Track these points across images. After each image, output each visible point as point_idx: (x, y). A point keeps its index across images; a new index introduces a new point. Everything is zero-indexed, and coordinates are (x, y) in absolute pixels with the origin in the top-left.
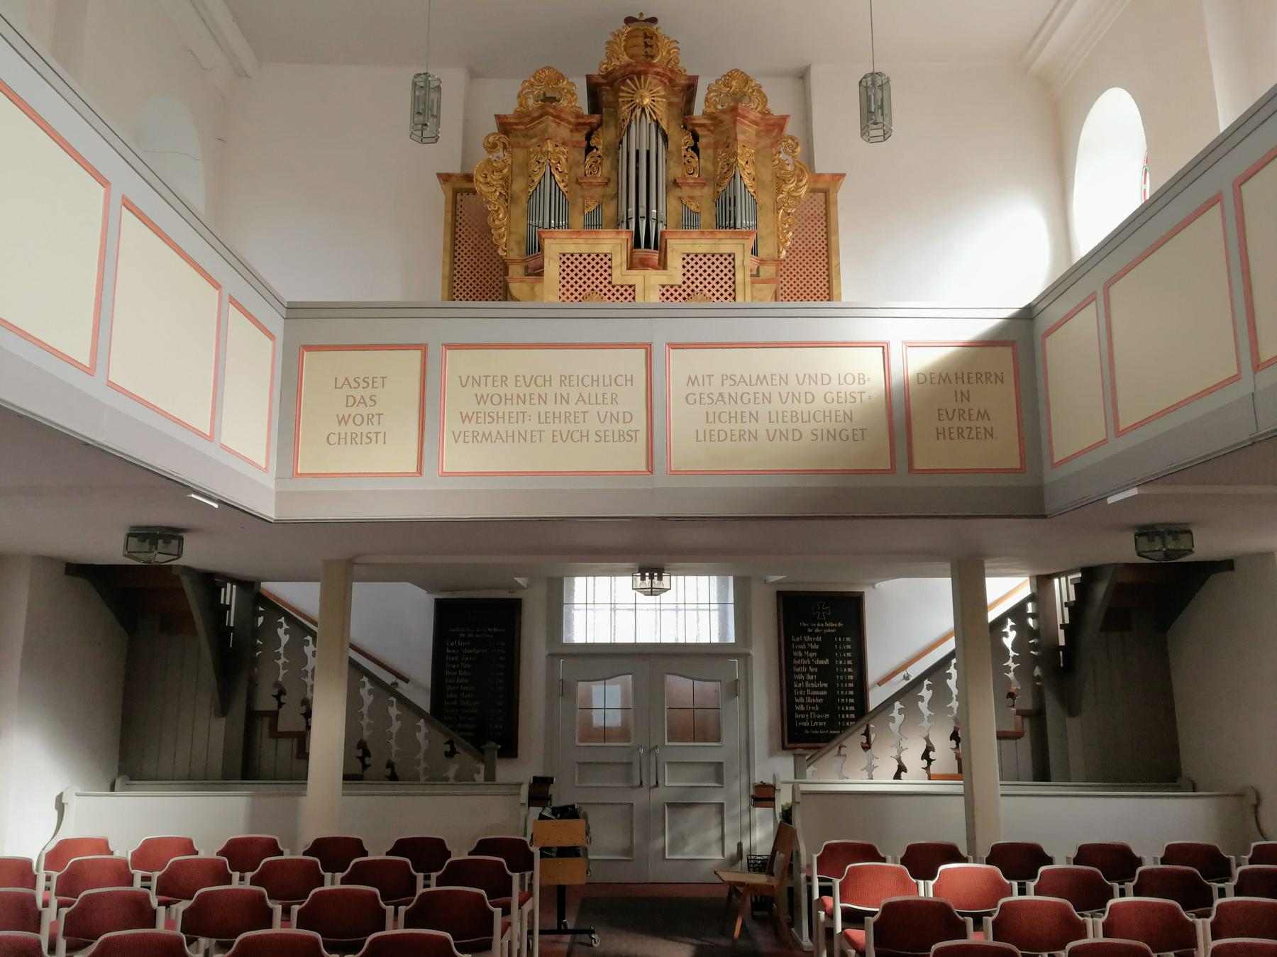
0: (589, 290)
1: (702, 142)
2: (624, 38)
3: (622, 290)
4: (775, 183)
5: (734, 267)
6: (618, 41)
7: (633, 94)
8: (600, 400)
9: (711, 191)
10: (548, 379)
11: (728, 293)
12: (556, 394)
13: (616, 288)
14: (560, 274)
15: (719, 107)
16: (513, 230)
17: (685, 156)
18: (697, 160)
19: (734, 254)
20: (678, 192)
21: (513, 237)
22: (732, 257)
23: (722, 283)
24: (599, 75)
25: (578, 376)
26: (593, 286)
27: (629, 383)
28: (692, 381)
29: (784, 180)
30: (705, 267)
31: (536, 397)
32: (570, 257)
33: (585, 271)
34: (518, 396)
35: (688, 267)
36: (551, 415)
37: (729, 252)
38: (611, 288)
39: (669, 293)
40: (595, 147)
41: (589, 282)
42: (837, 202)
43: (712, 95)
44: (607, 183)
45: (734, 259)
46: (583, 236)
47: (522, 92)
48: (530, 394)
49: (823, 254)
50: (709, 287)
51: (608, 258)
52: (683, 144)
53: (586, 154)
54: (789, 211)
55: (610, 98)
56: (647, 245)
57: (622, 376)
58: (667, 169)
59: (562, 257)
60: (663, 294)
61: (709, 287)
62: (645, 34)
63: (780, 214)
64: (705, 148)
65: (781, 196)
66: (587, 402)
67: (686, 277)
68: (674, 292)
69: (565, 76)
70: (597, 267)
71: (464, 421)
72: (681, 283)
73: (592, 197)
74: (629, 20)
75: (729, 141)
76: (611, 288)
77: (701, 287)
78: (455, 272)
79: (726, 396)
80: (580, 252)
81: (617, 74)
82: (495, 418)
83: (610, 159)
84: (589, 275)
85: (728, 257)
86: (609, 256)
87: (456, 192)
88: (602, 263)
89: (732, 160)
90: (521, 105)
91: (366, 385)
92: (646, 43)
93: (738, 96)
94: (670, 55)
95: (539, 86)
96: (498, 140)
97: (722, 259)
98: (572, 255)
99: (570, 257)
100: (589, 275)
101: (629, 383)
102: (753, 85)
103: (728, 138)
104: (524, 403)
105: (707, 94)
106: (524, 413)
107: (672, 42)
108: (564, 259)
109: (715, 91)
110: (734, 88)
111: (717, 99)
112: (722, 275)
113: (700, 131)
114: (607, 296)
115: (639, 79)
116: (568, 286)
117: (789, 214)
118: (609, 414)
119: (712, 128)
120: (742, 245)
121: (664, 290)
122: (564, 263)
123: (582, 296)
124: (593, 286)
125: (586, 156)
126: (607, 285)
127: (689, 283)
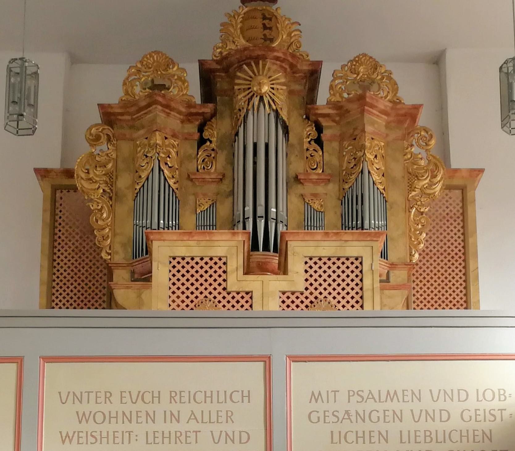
0: (201, 297)
1: (327, 134)
2: (240, 20)
3: (238, 297)
4: (406, 179)
5: (361, 272)
6: (234, 23)
7: (251, 81)
8: (214, 418)
10: (156, 394)
11: (355, 300)
12: (165, 412)
13: (231, 295)
14: (170, 279)
16: (118, 231)
17: (307, 150)
18: (321, 153)
19: (362, 257)
20: (299, 189)
21: (118, 239)
22: (360, 260)
23: (348, 289)
24: (213, 60)
25: (189, 392)
26: (206, 293)
27: (246, 399)
28: (315, 397)
29: (417, 176)
30: (330, 272)
31: (143, 415)
32: (181, 261)
33: (197, 276)
34: (124, 413)
35: (311, 272)
36: (159, 435)
38: (226, 295)
39: (290, 300)
40: (208, 139)
41: (202, 289)
42: (475, 200)
43: (337, 82)
44: (221, 179)
45: (361, 263)
46: (195, 238)
47: (127, 78)
48: (137, 412)
49: (460, 257)
50: (334, 294)
52: (306, 136)
54: (422, 210)
55: (225, 86)
56: (266, 248)
57: (238, 391)
58: (288, 164)
59: (172, 260)
60: (283, 302)
61: (334, 294)
63: (413, 213)
64: (330, 140)
65: (413, 193)
66: (200, 421)
67: (309, 282)
68: (295, 300)
69: (175, 60)
70: (211, 272)
71: (63, 442)
72: (303, 289)
73: (205, 195)
75: (356, 133)
76: (226, 295)
77: (325, 293)
78: (54, 277)
79: (353, 413)
80: (192, 255)
81: (233, 59)
82: (98, 438)
83: (225, 152)
84: (202, 280)
85: (355, 261)
86: (224, 260)
87: (55, 189)
88: (216, 268)
89: (360, 154)
90: (127, 93)
93: (366, 83)
94: (291, 38)
95: (146, 72)
96: (101, 132)
97: (348, 263)
98: (183, 259)
99: (181, 261)
100: (202, 280)
101: (246, 399)
102: (383, 71)
103: (355, 129)
104: (130, 421)
105: (332, 81)
106: (130, 433)
108: (174, 263)
109: (341, 78)
111: (343, 87)
112: (348, 280)
113: (324, 122)
114: (222, 304)
115: (257, 64)
116: (179, 293)
117: (422, 213)
118: (224, 434)
119: (337, 119)
120: (369, 248)
121: (284, 298)
123: (194, 303)
124: (206, 293)
125: (198, 149)
126: (222, 291)
127: (312, 289)
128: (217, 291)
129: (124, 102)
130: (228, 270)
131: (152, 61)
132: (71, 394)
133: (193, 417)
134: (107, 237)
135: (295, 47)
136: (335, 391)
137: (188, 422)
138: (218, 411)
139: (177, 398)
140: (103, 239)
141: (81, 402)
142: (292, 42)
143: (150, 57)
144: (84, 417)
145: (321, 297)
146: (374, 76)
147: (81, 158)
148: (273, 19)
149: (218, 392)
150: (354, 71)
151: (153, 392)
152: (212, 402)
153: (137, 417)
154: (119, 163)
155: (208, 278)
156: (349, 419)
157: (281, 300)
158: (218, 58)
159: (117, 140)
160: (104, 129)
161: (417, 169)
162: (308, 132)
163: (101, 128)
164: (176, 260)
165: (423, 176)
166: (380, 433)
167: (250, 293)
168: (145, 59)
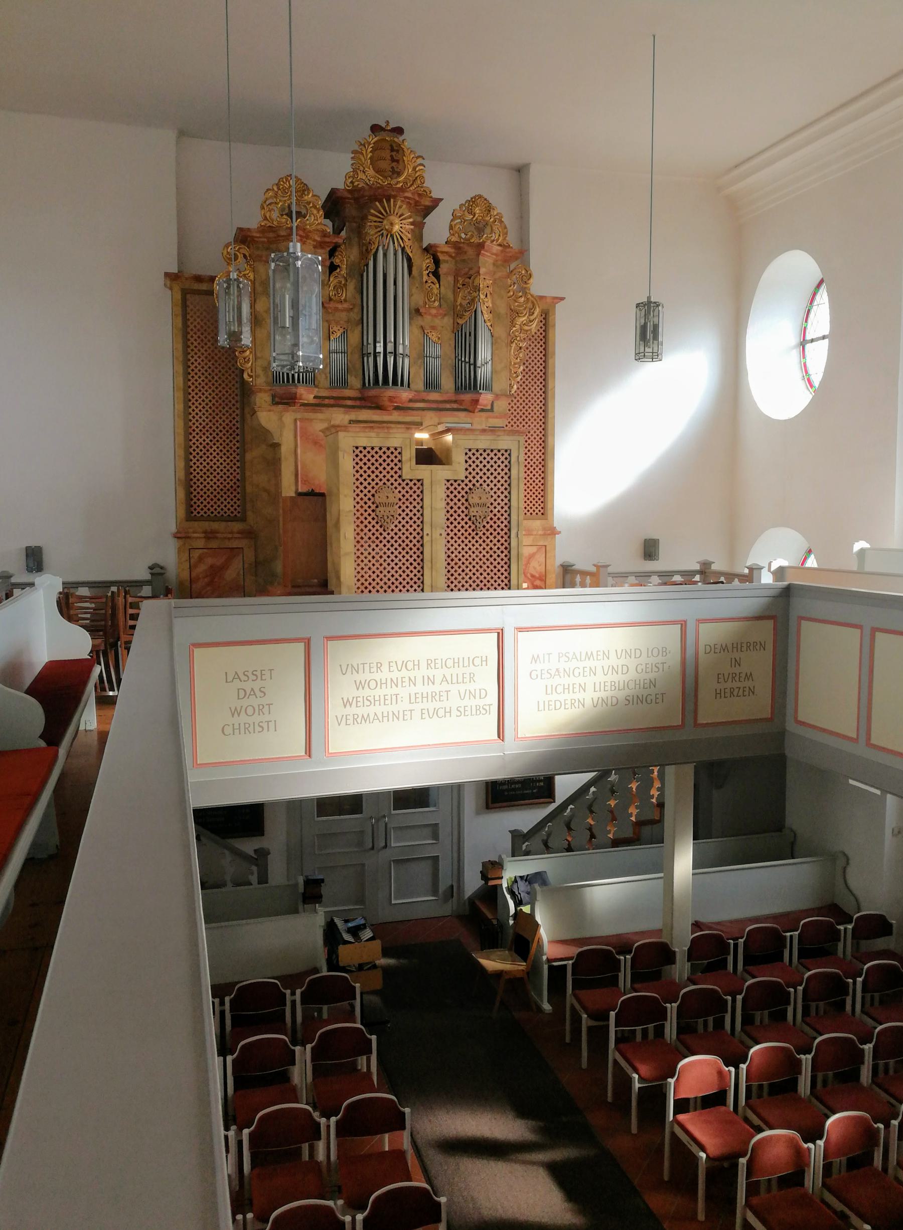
0: (381, 484)
1: (444, 268)
3: (411, 484)
5: (509, 462)
6: (364, 152)
8: (460, 680)
9: (452, 321)
10: (416, 663)
11: (504, 487)
13: (405, 482)
15: (463, 236)
16: (259, 355)
17: (426, 282)
20: (419, 321)
21: (259, 362)
22: (508, 452)
23: (499, 478)
24: (345, 189)
26: (384, 480)
27: (484, 663)
28: (535, 659)
30: (485, 462)
31: (407, 680)
32: (363, 450)
33: (377, 464)
34: (392, 680)
35: (470, 462)
36: (419, 696)
37: (506, 448)
38: (401, 482)
39: (453, 487)
40: (339, 266)
41: (381, 476)
46: (376, 430)
47: (265, 202)
49: (541, 377)
50: (488, 481)
51: (398, 451)
52: (424, 268)
53: (330, 273)
55: (354, 213)
56: (395, 383)
58: (411, 295)
59: (355, 449)
60: (448, 489)
61: (488, 481)
62: (391, 146)
64: (446, 274)
65: (514, 329)
66: (450, 682)
67: (468, 471)
68: (457, 487)
69: (310, 186)
70: (388, 461)
71: (345, 706)
72: (464, 478)
73: (337, 323)
74: (375, 129)
75: (471, 272)
76: (401, 482)
77: (481, 481)
78: (190, 383)
79: (562, 670)
82: (373, 701)
83: (354, 281)
84: (381, 468)
85: (504, 453)
86: (399, 450)
87: (185, 293)
88: (392, 457)
89: (475, 294)
90: (265, 218)
91: (255, 678)
92: (391, 156)
93: (481, 225)
94: (416, 172)
96: (238, 251)
97: (499, 455)
98: (365, 448)
99: (363, 450)
100: (381, 468)
101: (484, 663)
102: (495, 213)
103: (471, 269)
104: (397, 686)
105: (452, 221)
106: (396, 695)
107: (418, 157)
108: (357, 452)
109: (460, 217)
110: (477, 216)
113: (441, 257)
114: (398, 490)
115: (388, 201)
116: (361, 479)
117: (521, 348)
118: (468, 692)
119: (453, 255)
120: (517, 442)
121: (448, 484)
122: (357, 456)
123: (375, 490)
124: (384, 480)
127: (470, 477)
132: (350, 666)
135: (419, 182)
142: (416, 178)
145: (478, 485)
146: (488, 219)
148: (401, 152)
150: (471, 212)
154: (257, 284)
160: (240, 248)
161: (518, 305)
162: (427, 263)
164: (359, 450)
165: (522, 313)
166: (580, 685)
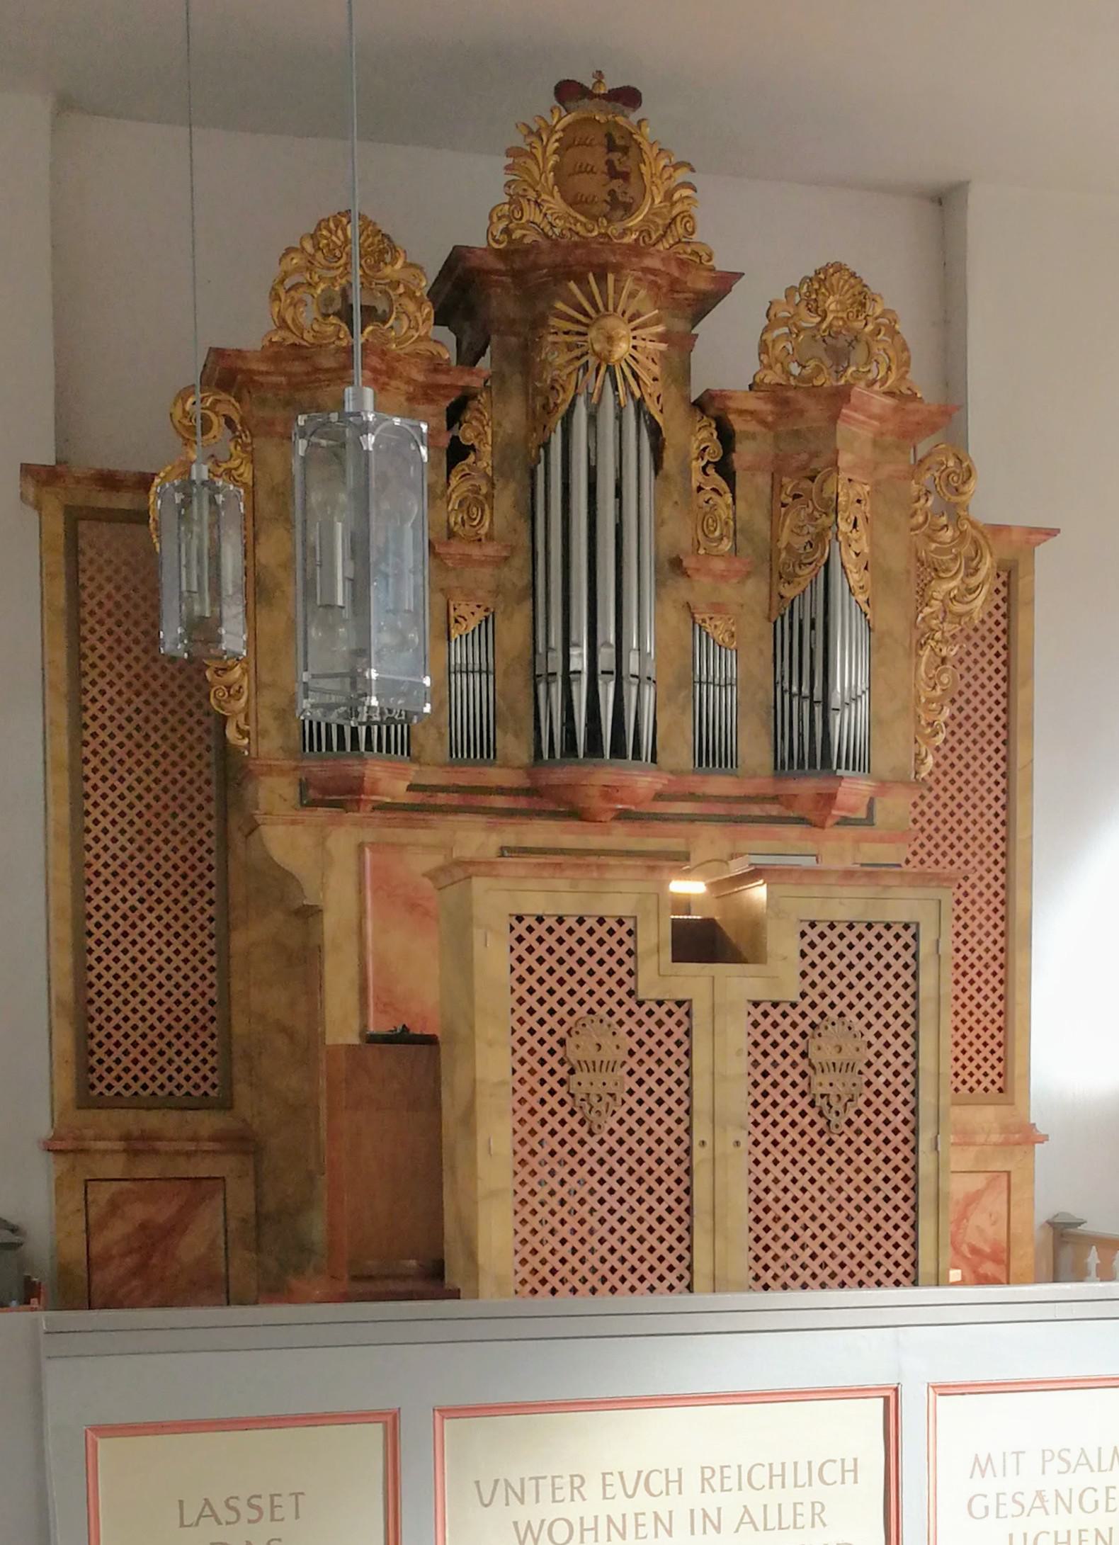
0: (581, 1011)
1: (744, 454)
2: (553, 146)
3: (660, 1013)
4: (913, 575)
5: (915, 956)
6: (539, 153)
7: (587, 325)
8: (788, 1519)
9: (766, 590)
10: (673, 1476)
11: (900, 1021)
12: (692, 1511)
13: (645, 1008)
14: (512, 969)
15: (795, 369)
16: (265, 677)
17: (700, 489)
18: (730, 501)
19: (918, 925)
20: (681, 590)
21: (267, 698)
22: (912, 930)
24: (489, 249)
25: (739, 1467)
26: (591, 1003)
28: (981, 1466)
29: (936, 570)
30: (851, 956)
31: (649, 1520)
32: (535, 924)
33: (571, 962)
34: (610, 1520)
37: (906, 919)
38: (635, 1008)
40: (472, 447)
41: (582, 992)
42: (1033, 600)
43: (777, 332)
44: (506, 558)
45: (915, 937)
46: (568, 873)
47: (282, 282)
48: (636, 1515)
50: (860, 1006)
51: (625, 928)
52: (695, 453)
53: (451, 466)
54: (944, 653)
57: (834, 1461)
58: (659, 524)
59: (515, 923)
60: (755, 1024)
61: (860, 1006)
62: (609, 137)
63: (924, 659)
65: (927, 610)
67: (808, 980)
68: (780, 1019)
69: (397, 241)
70: (601, 952)
72: (797, 999)
73: (469, 595)
74: (567, 92)
75: (815, 464)
76: (635, 1008)
77: (842, 1005)
79: (1050, 1496)
80: (560, 913)
81: (545, 259)
83: (512, 486)
85: (902, 932)
86: (629, 924)
87: (75, 517)
88: (611, 942)
89: (825, 521)
90: (283, 324)
91: (254, 1514)
92: (610, 163)
93: (841, 343)
94: (673, 204)
95: (329, 269)
97: (888, 937)
98: (540, 920)
99: (535, 924)
100: (581, 972)
102: (878, 311)
103: (815, 455)
104: (623, 1536)
105: (766, 330)
107: (677, 166)
108: (521, 929)
110: (830, 317)
111: (789, 347)
112: (888, 976)
113: (738, 424)
114: (625, 1028)
115: (601, 279)
116: (531, 1001)
117: (944, 660)
119: (770, 419)
120: (934, 905)
121: (757, 1014)
122: (520, 939)
123: (566, 1027)
124: (591, 1003)
125: (449, 473)
126: (625, 998)
127: (813, 995)
128: (616, 998)
129: (275, 349)
130: (639, 950)
131: (342, 238)
132: (502, 1484)
133: (746, 1519)
134: (239, 691)
135: (681, 231)
136: (1018, 1453)
137: (737, 1531)
138: (795, 1504)
139: (716, 1482)
140: (230, 695)
141: (522, 1501)
142: (674, 219)
143: (337, 227)
144: (529, 1533)
145: (833, 1015)
146: (859, 325)
147: (162, 474)
148: (633, 151)
149: (796, 1463)
150: (814, 307)
151: (667, 1470)
152: (783, 1486)
153: (637, 1525)
154: (261, 495)
155: (596, 967)
156: (1044, 1507)
157: (751, 1019)
158: (501, 246)
159: (252, 436)
160: (217, 401)
161: (936, 551)
162: (703, 441)
163: (210, 400)
164: (525, 924)
165: (947, 570)
166: (1098, 1533)
167: (686, 1005)
168: (325, 232)
